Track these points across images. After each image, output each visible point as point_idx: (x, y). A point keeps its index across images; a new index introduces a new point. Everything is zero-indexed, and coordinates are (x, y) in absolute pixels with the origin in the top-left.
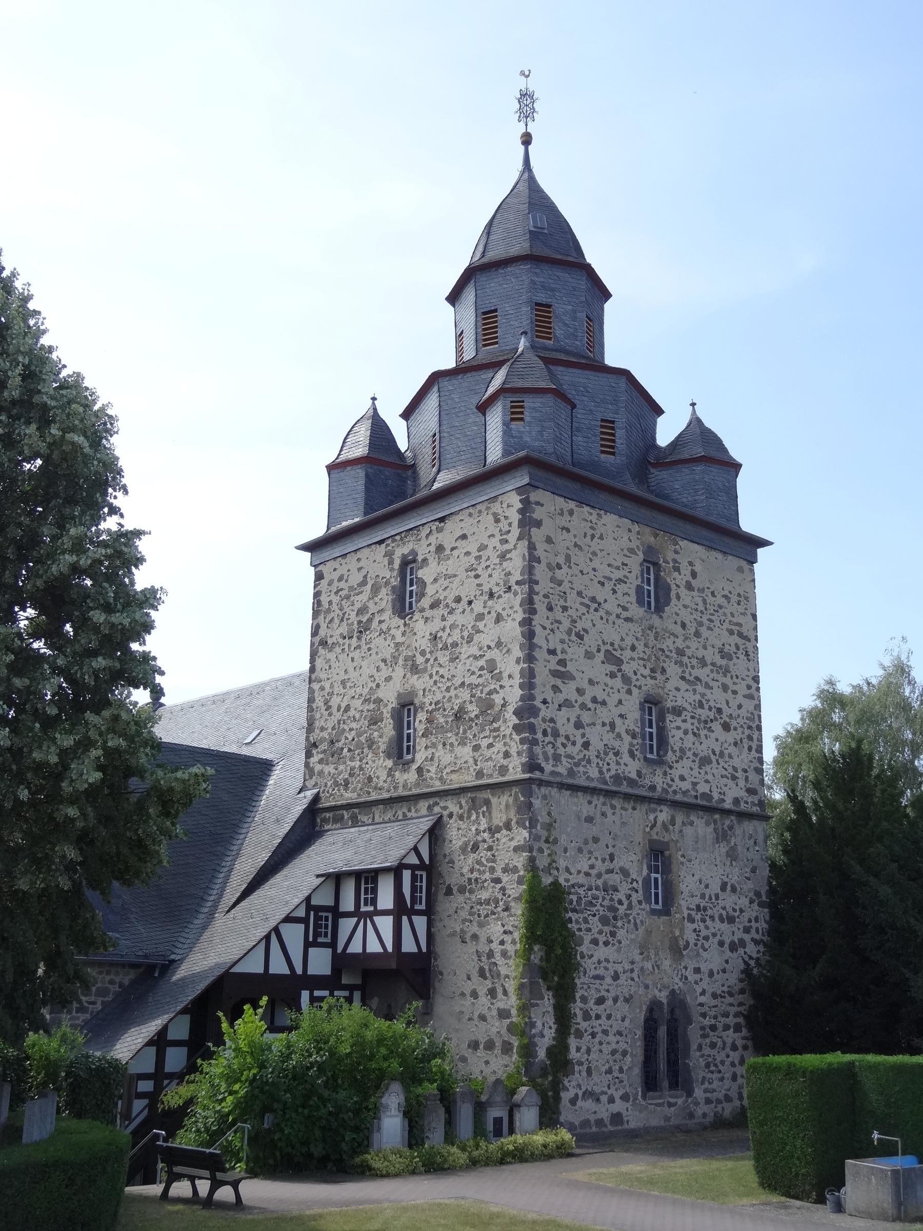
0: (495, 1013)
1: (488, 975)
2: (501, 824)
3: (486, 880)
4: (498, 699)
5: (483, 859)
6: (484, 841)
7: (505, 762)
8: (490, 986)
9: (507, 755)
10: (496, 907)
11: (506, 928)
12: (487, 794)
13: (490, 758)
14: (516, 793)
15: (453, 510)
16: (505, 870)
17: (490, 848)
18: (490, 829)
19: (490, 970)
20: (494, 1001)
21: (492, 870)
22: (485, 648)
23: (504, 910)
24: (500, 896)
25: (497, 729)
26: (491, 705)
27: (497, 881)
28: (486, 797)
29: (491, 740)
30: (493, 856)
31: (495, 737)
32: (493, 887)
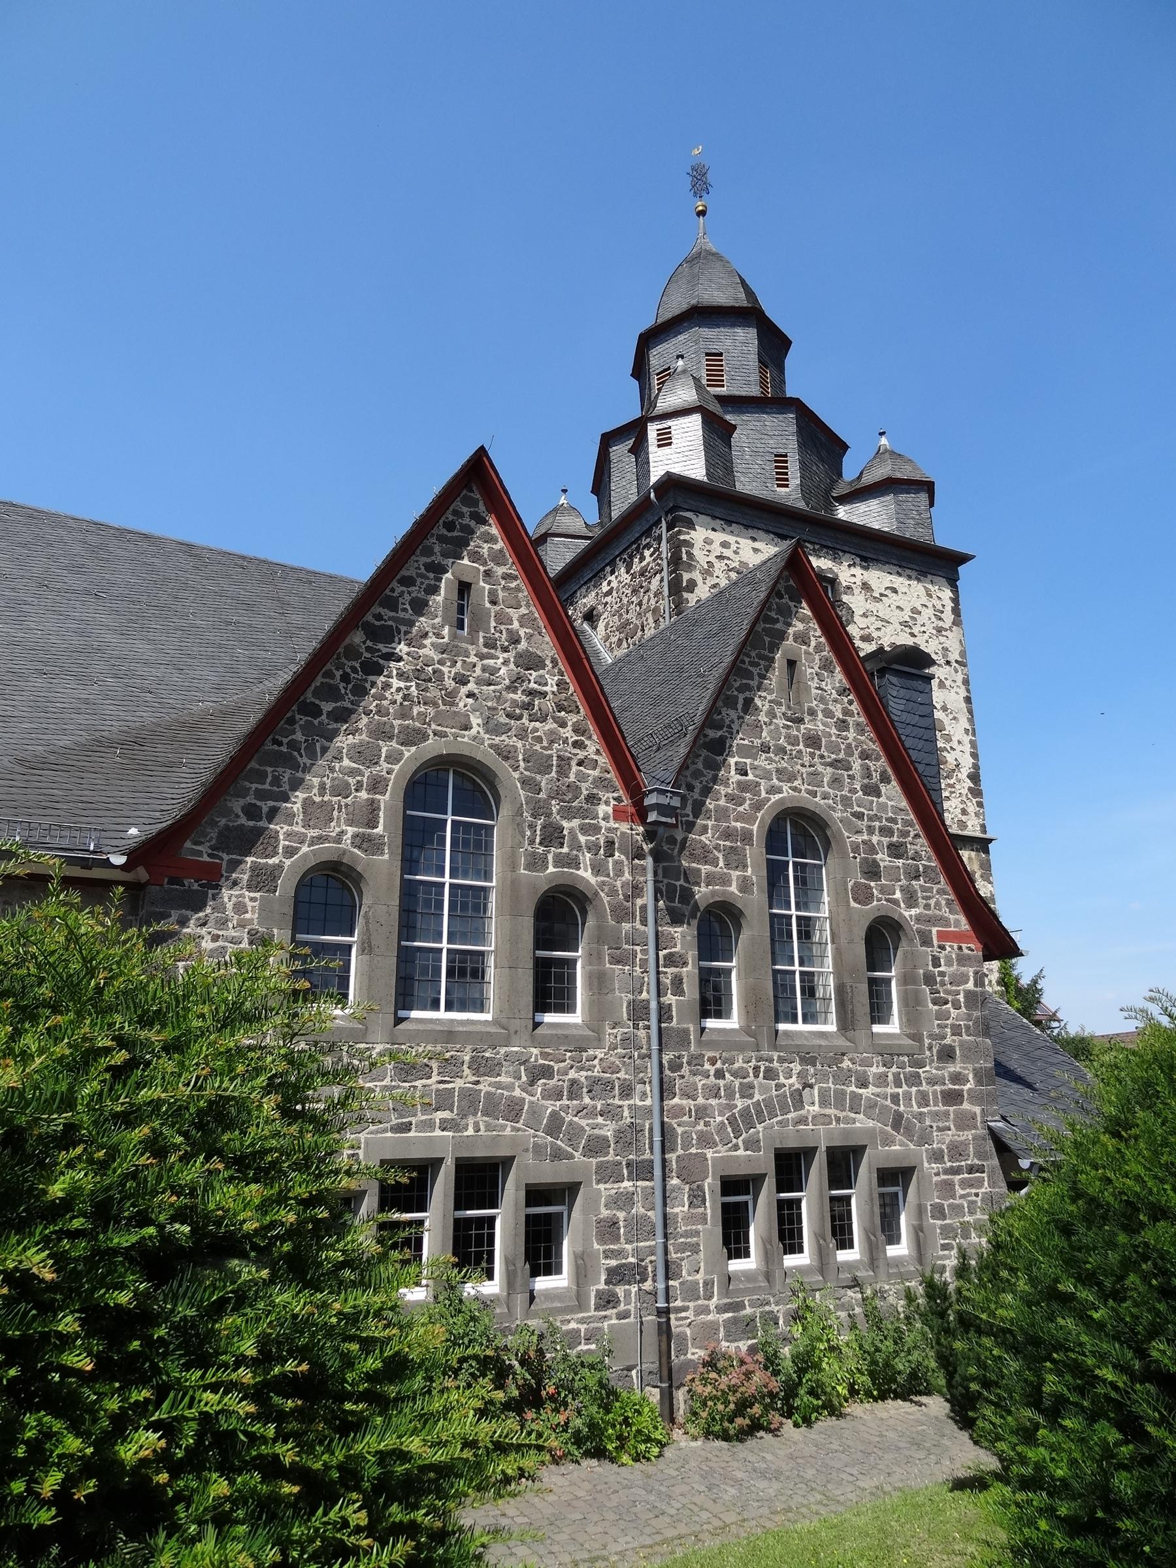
7: (964, 818)
9: (964, 812)
15: (881, 558)
31: (952, 793)
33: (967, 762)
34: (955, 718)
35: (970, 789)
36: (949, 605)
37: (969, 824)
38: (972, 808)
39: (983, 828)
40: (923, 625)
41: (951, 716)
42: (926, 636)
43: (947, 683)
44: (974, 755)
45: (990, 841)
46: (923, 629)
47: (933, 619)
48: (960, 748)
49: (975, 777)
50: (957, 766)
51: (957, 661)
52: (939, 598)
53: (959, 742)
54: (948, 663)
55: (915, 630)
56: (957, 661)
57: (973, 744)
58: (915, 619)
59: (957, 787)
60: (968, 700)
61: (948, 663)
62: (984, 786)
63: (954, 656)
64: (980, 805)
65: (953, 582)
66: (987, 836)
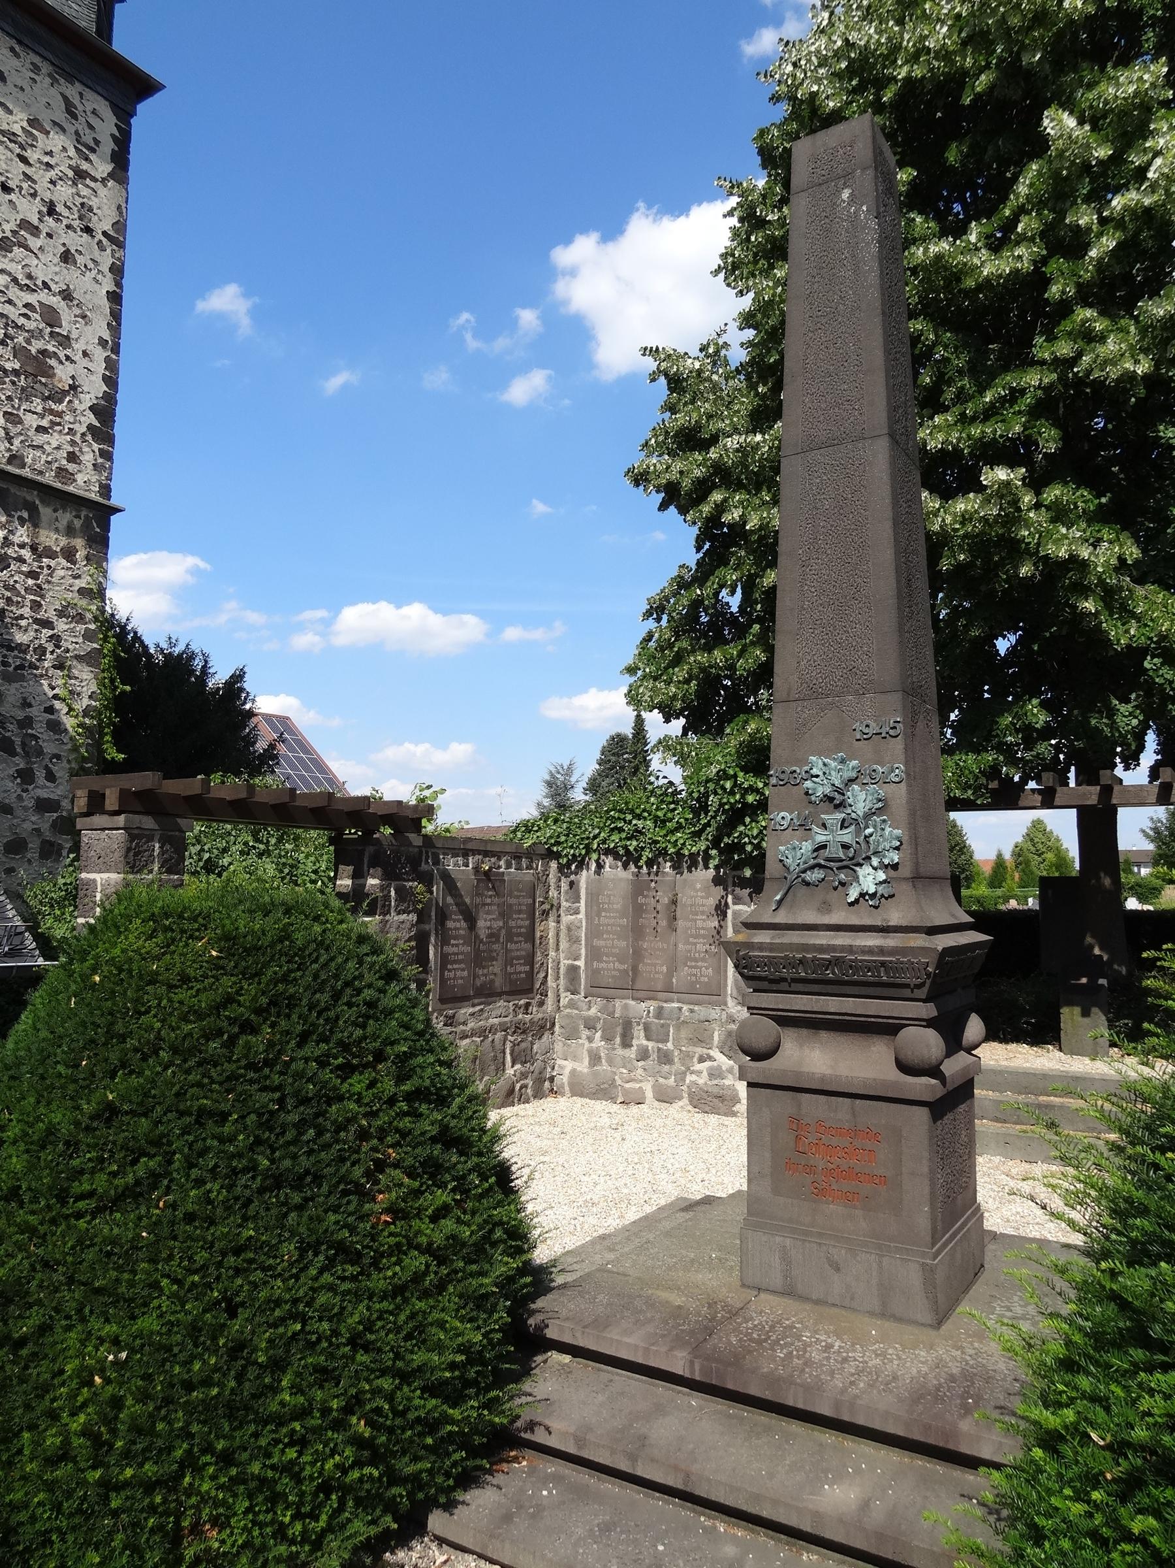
0: (30, 803)
1: (19, 750)
2: (58, 549)
3: (22, 617)
4: (63, 374)
5: (17, 586)
6: (21, 560)
7: (71, 467)
8: (22, 766)
9: (72, 457)
10: (39, 660)
11: (56, 691)
12: (33, 497)
13: (40, 447)
14: (87, 517)
16: (61, 614)
17: (33, 575)
18: (34, 549)
19: (24, 744)
20: (30, 788)
21: (36, 606)
22: (39, 283)
23: (54, 667)
24: (50, 647)
25: (60, 414)
26: (49, 372)
27: (47, 624)
28: (29, 498)
29: (45, 423)
30: (39, 586)
31: (53, 424)
32: (36, 631)
33: (93, 389)
34: (84, 317)
35: (90, 427)
36: (108, 146)
37: (80, 478)
38: (88, 458)
39: (106, 490)
40: (50, 153)
41: (78, 311)
42: (52, 174)
43: (80, 260)
44: (111, 381)
45: (117, 510)
46: (46, 159)
47: (72, 152)
48: (85, 362)
49: (105, 411)
50: (73, 387)
51: (105, 234)
52: (91, 127)
53: (85, 354)
54: (88, 230)
55: (33, 155)
56: (105, 234)
57: (112, 366)
58: (35, 138)
59: (68, 418)
60: (115, 298)
61: (88, 230)
62: (118, 430)
63: (104, 223)
64: (107, 456)
65: (124, 115)
66: (114, 501)
